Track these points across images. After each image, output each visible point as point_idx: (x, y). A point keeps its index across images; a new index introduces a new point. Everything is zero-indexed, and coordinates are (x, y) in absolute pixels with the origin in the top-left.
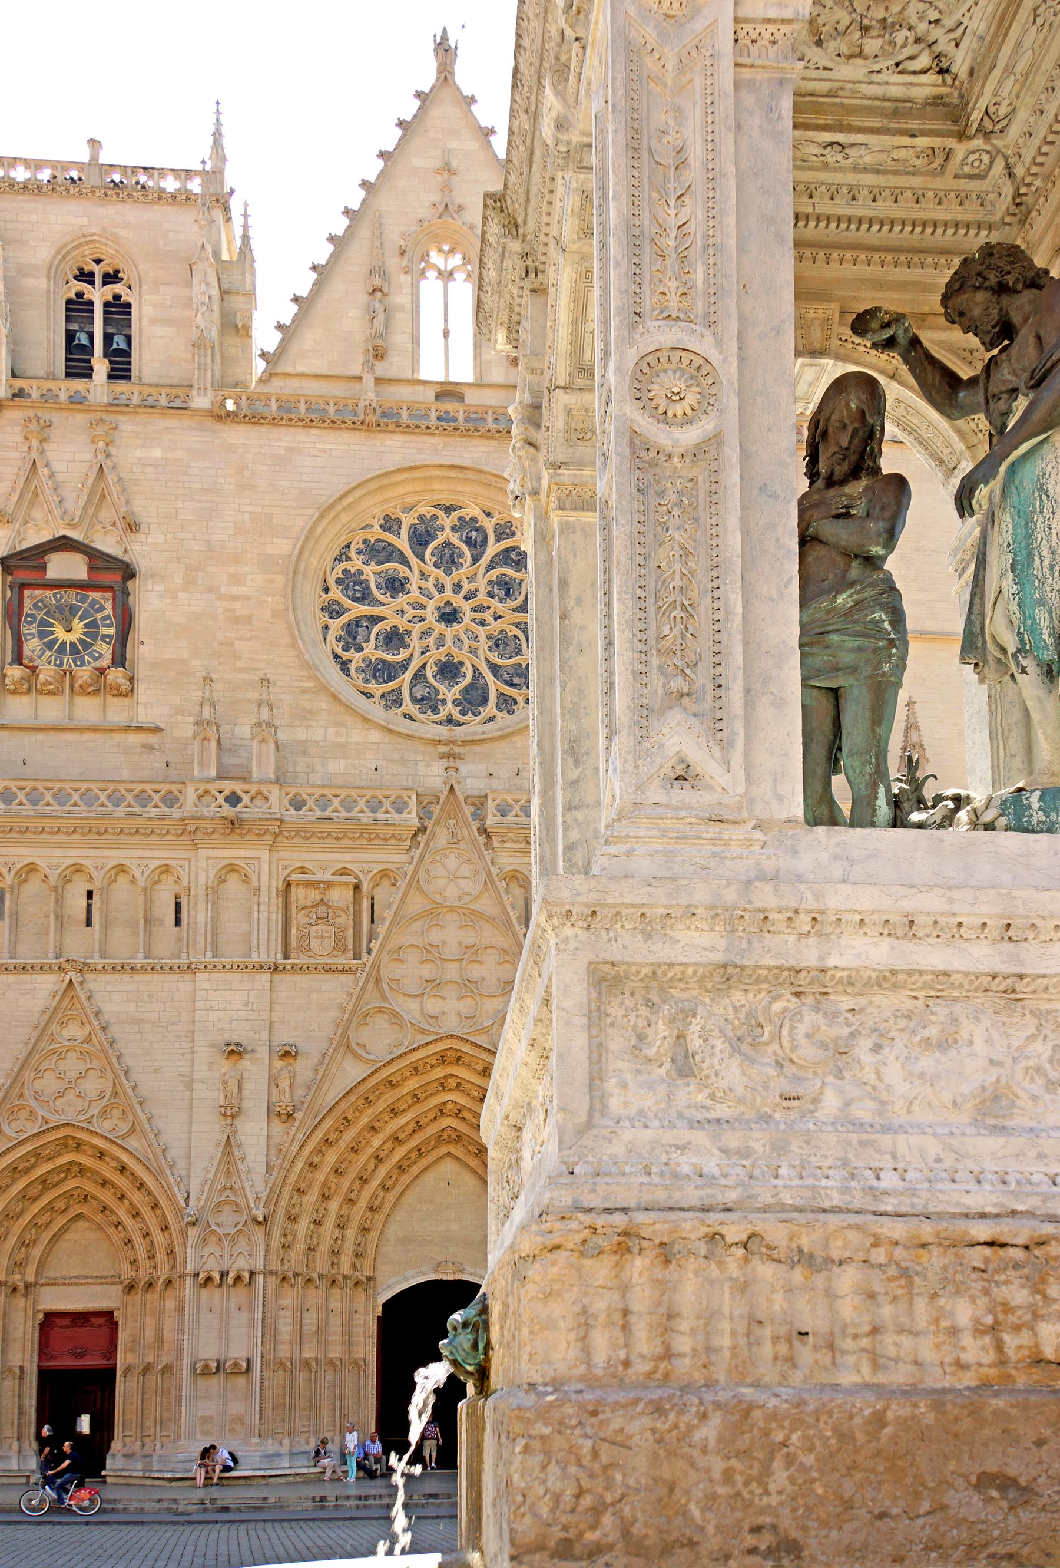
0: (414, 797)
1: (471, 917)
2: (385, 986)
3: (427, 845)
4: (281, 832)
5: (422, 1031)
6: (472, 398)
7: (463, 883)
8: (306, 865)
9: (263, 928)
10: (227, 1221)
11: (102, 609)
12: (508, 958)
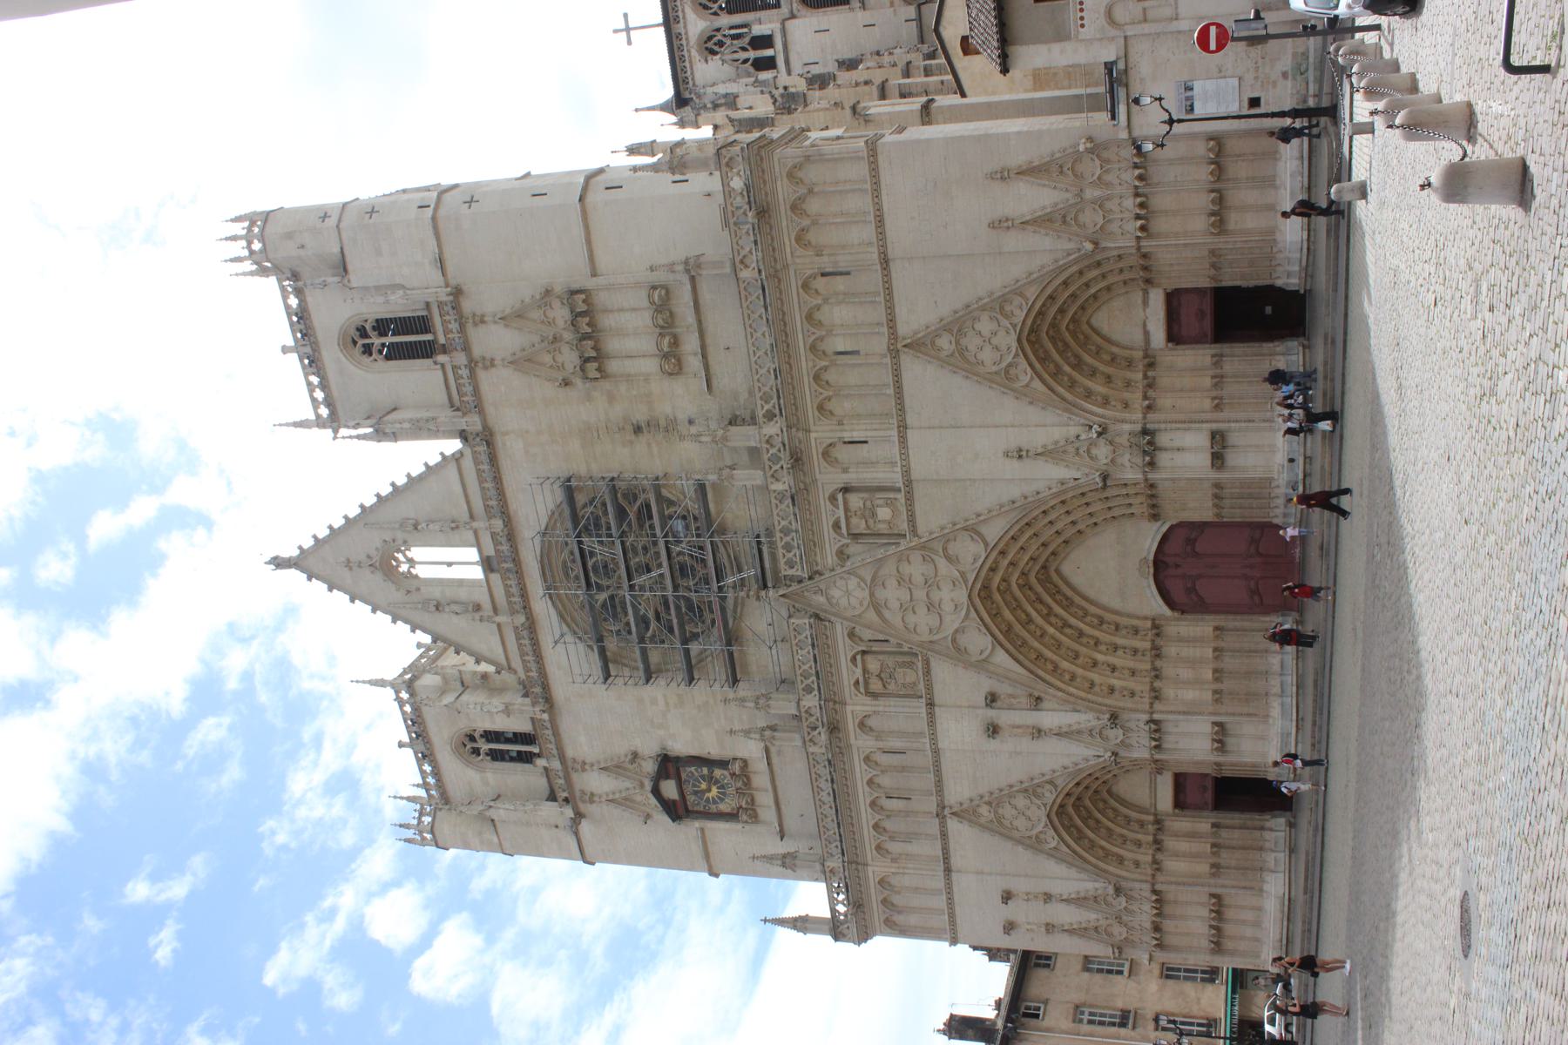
0: (792, 620)
1: (875, 583)
2: (935, 638)
3: (826, 611)
4: (831, 700)
5: (968, 611)
6: (490, 551)
7: (851, 587)
8: (852, 683)
9: (901, 710)
10: (1116, 735)
11: (691, 772)
12: (904, 558)
